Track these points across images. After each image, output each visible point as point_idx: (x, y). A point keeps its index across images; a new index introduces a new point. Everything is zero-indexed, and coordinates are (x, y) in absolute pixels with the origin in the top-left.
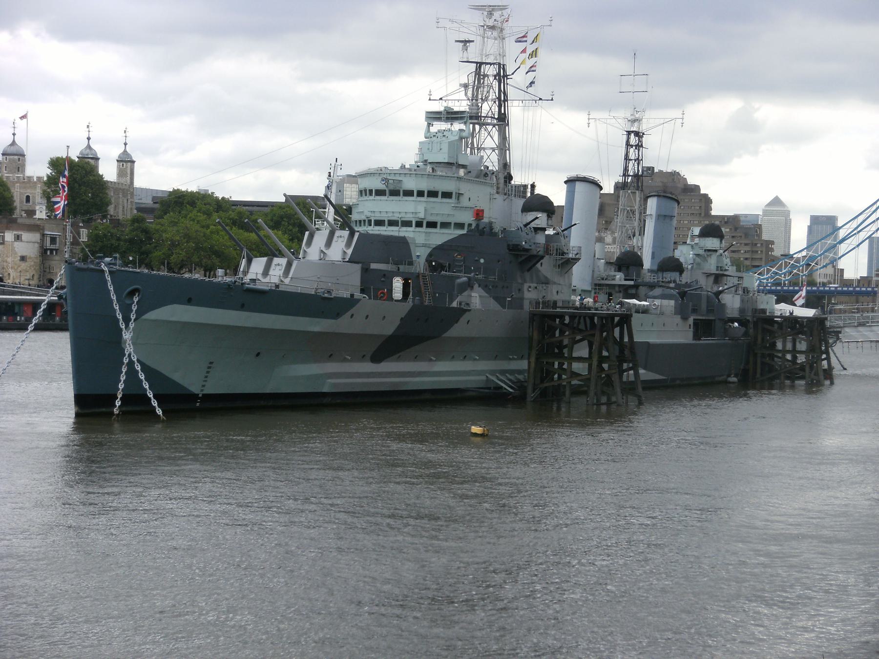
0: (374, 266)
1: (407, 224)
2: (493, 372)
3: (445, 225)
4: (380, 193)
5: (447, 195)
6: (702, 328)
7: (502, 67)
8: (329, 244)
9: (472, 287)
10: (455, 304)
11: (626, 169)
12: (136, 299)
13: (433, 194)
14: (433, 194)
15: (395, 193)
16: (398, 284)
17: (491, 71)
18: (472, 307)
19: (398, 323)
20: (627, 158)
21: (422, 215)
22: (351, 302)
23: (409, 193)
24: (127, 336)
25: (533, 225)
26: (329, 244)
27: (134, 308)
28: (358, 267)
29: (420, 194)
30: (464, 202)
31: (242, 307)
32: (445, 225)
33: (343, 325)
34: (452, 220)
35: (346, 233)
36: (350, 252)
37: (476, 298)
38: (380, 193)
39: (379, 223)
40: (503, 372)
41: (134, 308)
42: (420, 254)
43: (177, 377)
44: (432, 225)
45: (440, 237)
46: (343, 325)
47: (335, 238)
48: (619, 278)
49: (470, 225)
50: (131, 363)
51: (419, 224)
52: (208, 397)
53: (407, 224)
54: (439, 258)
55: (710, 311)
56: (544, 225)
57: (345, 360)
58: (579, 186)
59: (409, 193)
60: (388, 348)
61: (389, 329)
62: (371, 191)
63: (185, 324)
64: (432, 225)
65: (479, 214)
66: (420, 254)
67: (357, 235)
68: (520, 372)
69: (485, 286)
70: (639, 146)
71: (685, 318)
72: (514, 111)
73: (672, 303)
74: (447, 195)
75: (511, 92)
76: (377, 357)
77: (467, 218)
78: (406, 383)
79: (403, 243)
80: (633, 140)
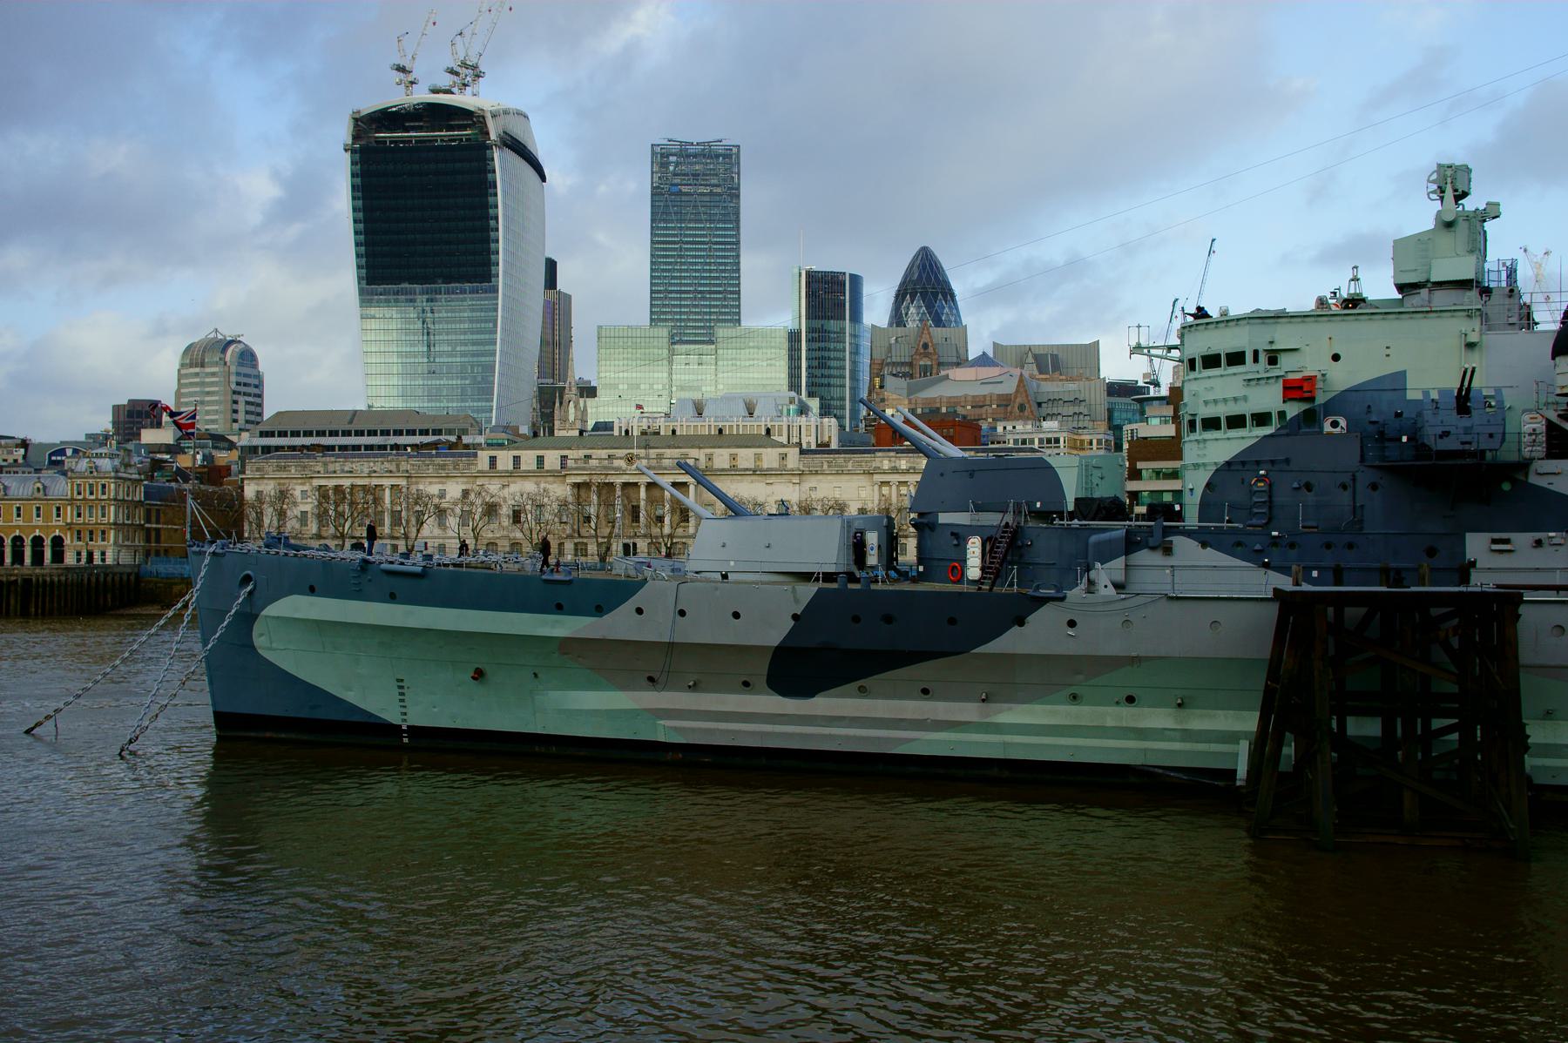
0: (944, 518)
3: (1236, 422)
5: (1236, 358)
9: (1168, 550)
16: (974, 547)
30: (1286, 363)
31: (392, 598)
32: (1236, 422)
33: (619, 624)
34: (1246, 409)
43: (351, 697)
44: (1212, 424)
45: (1224, 447)
46: (619, 624)
49: (1282, 414)
57: (694, 688)
63: (320, 626)
64: (1212, 424)
65: (1296, 389)
77: (1269, 398)
78: (888, 740)
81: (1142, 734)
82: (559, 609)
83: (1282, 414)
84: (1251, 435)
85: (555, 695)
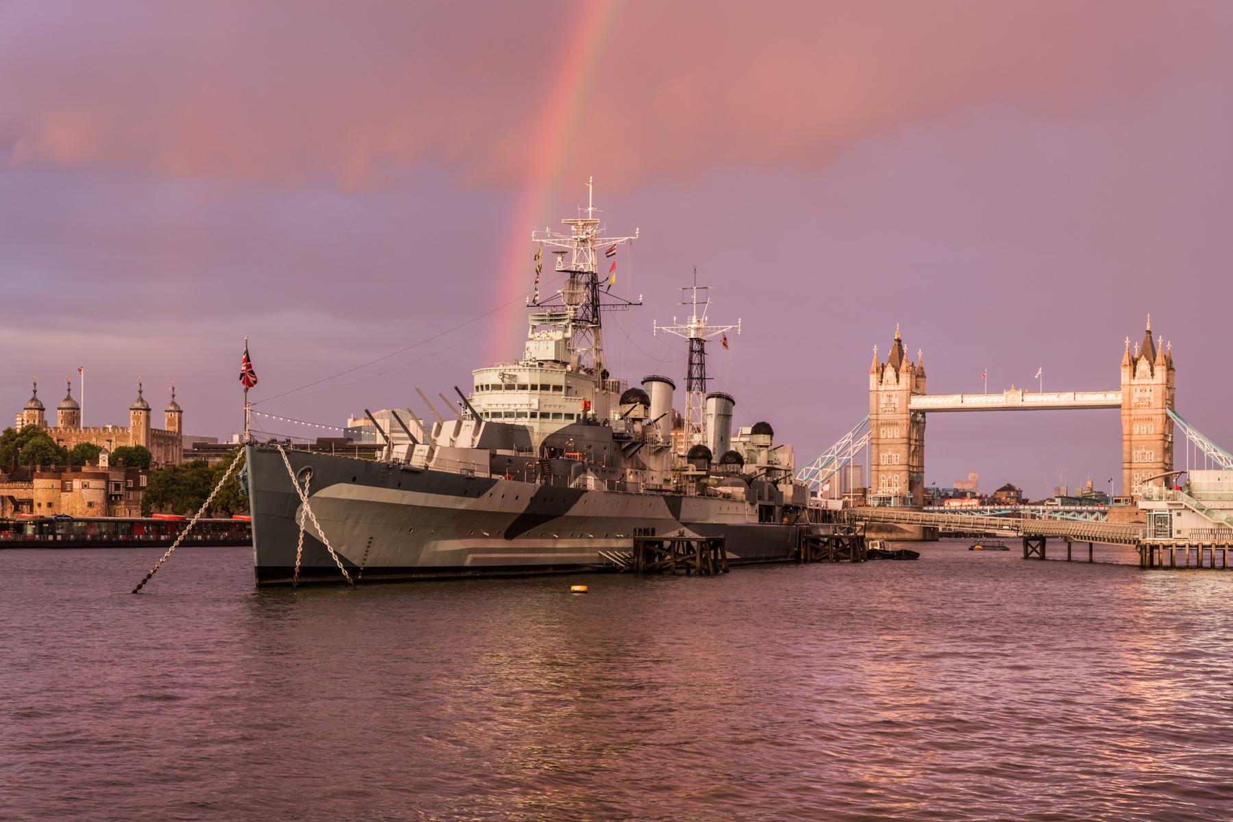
0: (499, 452)
1: (520, 415)
2: (604, 550)
3: (557, 415)
4: (496, 387)
5: (557, 388)
6: (765, 513)
7: (594, 276)
8: (457, 433)
10: (572, 486)
11: (690, 373)
12: (308, 478)
13: (545, 387)
14: (545, 387)
15: (510, 387)
17: (584, 279)
18: (589, 487)
19: (528, 502)
20: (691, 363)
21: (536, 406)
22: (489, 483)
23: (524, 387)
24: (306, 507)
25: (632, 415)
26: (457, 433)
27: (307, 486)
28: (488, 452)
29: (534, 387)
31: (399, 486)
34: (563, 411)
35: (474, 423)
36: (478, 438)
37: (591, 481)
38: (496, 387)
39: (495, 415)
40: (612, 549)
41: (307, 486)
42: (537, 441)
43: (342, 551)
44: (544, 415)
45: (554, 426)
47: (463, 427)
48: (692, 470)
49: (579, 416)
50: (307, 536)
51: (533, 415)
52: (369, 571)
53: (520, 415)
54: (553, 446)
55: (770, 498)
56: (642, 416)
58: (656, 386)
59: (524, 387)
60: (519, 526)
61: (521, 507)
62: (487, 386)
63: (352, 503)
64: (544, 415)
65: (587, 406)
66: (537, 441)
67: (483, 424)
68: (626, 550)
69: (596, 472)
70: (702, 352)
71: (752, 504)
72: (604, 315)
73: (742, 489)
74: (557, 388)
75: (604, 298)
76: (510, 534)
77: (576, 408)
79: (524, 431)
80: (696, 347)
81: (582, 550)
82: (465, 493)
83: (579, 416)
84: (562, 424)
85: (432, 544)
